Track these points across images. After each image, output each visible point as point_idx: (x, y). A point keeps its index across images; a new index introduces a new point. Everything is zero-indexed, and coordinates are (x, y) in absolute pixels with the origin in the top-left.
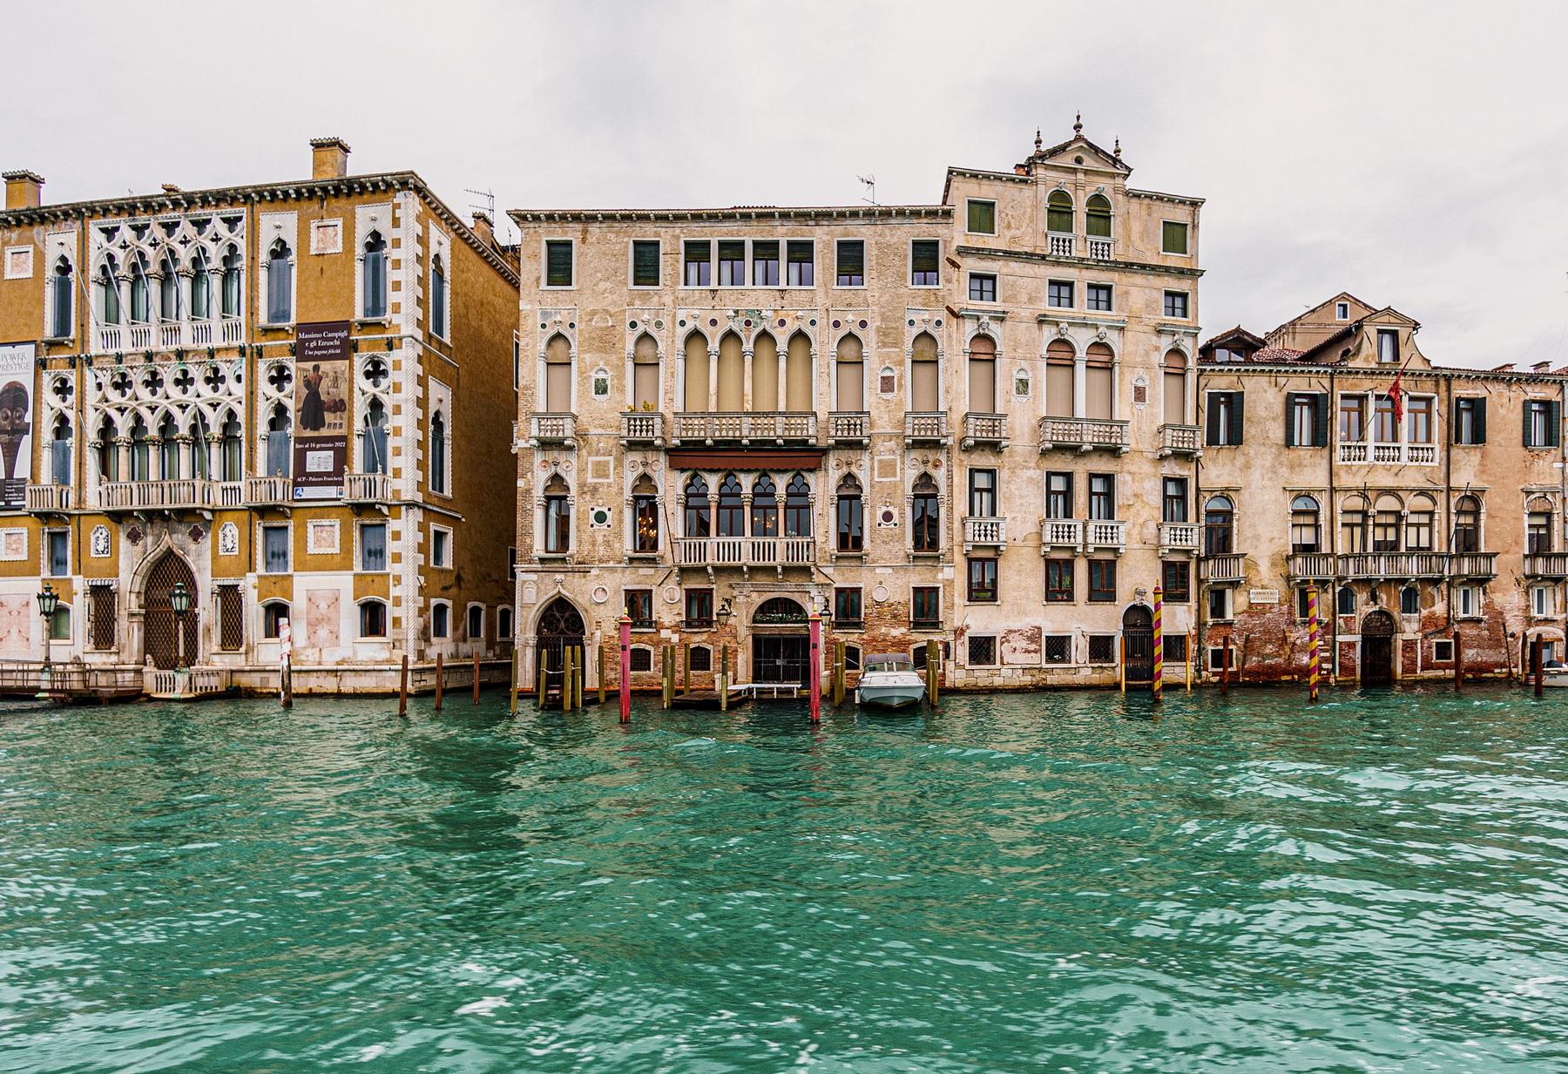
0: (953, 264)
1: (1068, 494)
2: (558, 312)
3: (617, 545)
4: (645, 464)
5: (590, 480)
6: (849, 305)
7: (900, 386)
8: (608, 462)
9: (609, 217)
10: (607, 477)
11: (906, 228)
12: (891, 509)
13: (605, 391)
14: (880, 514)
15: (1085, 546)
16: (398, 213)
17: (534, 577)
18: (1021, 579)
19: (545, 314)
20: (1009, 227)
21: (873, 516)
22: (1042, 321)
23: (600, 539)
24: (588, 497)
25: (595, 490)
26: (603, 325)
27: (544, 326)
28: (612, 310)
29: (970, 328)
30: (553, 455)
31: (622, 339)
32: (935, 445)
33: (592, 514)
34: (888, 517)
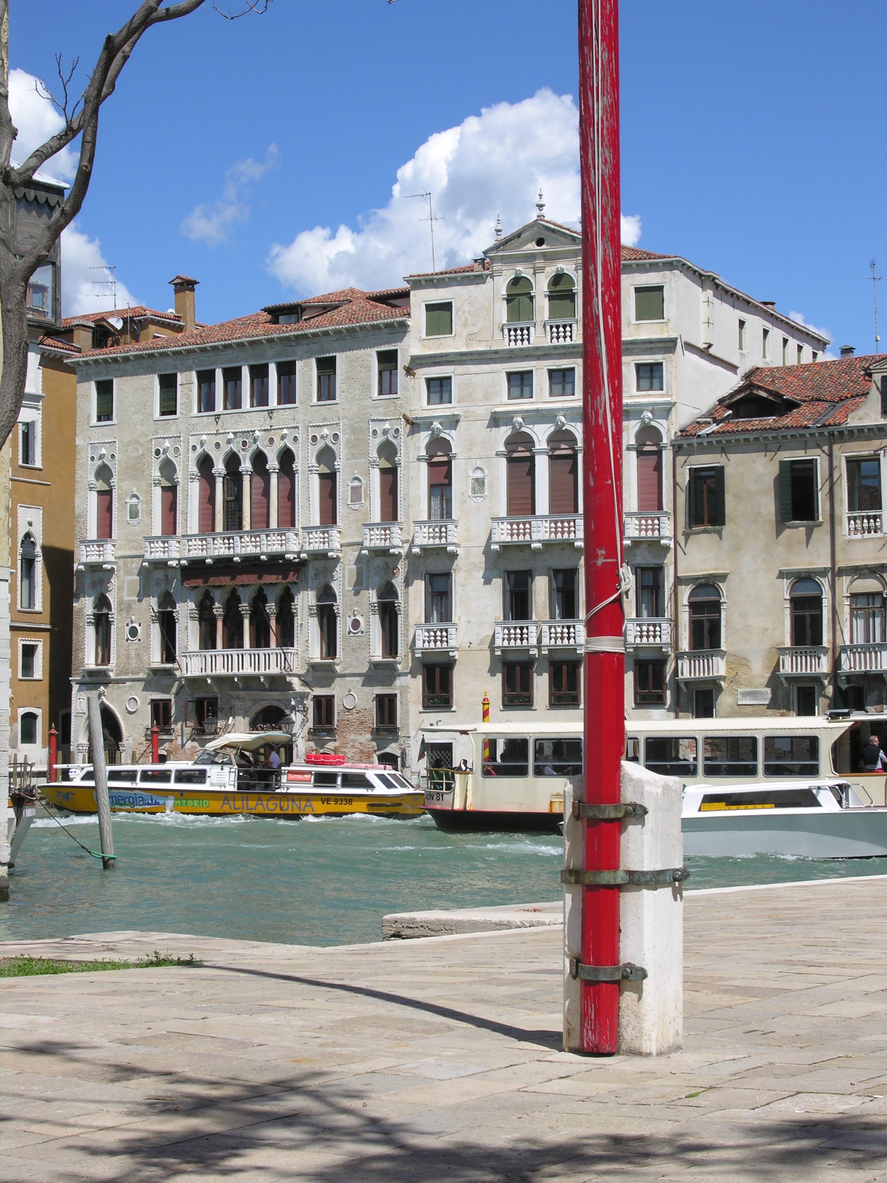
3: (145, 658)
5: (126, 598)
6: (324, 419)
12: (358, 617)
14: (349, 621)
18: (477, 683)
20: (465, 324)
21: (345, 623)
22: (496, 420)
23: (133, 653)
24: (124, 614)
26: (134, 454)
27: (93, 459)
28: (142, 440)
29: (424, 437)
34: (356, 624)
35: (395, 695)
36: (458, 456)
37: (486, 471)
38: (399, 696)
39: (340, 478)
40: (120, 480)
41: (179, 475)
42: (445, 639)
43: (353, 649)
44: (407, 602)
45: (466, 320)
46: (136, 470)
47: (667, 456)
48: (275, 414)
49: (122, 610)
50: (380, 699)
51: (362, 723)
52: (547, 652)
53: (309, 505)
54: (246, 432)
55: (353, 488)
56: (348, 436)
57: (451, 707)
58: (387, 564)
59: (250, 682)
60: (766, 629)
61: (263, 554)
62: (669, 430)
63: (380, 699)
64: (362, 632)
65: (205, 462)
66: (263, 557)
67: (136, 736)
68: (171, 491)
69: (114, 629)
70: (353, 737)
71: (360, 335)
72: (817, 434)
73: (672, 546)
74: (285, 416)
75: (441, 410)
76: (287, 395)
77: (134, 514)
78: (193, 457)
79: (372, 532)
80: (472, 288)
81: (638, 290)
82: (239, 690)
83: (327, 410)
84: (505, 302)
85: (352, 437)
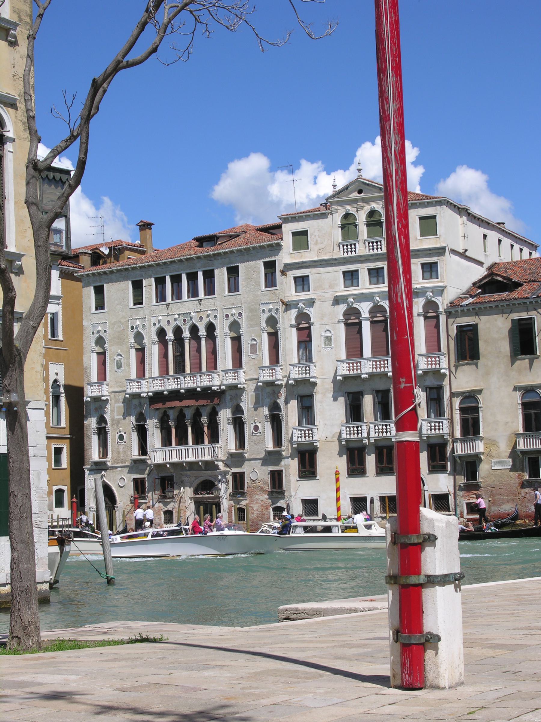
3: (129, 453)
5: (116, 417)
6: (233, 304)
14: (252, 426)
18: (331, 462)
20: (316, 243)
21: (249, 428)
22: (337, 301)
23: (121, 450)
24: (115, 427)
26: (119, 329)
27: (93, 333)
28: (123, 321)
29: (293, 313)
34: (256, 428)
35: (282, 470)
36: (315, 324)
37: (332, 332)
38: (284, 471)
40: (110, 346)
41: (146, 341)
42: (311, 435)
44: (287, 413)
45: (317, 241)
47: (443, 319)
48: (203, 302)
49: (114, 424)
50: (272, 473)
51: (262, 488)
52: (373, 441)
53: (225, 357)
54: (185, 313)
55: (251, 345)
56: (247, 314)
57: (316, 477)
58: (274, 391)
59: (193, 465)
60: (507, 423)
61: (198, 387)
62: (443, 303)
63: (272, 473)
64: (260, 433)
65: (161, 333)
66: (198, 389)
67: (125, 501)
68: (141, 351)
69: (109, 436)
70: (257, 497)
71: (252, 252)
72: (534, 302)
73: (448, 374)
74: (209, 303)
75: (304, 296)
76: (210, 290)
77: (119, 366)
78: (154, 330)
79: (264, 372)
80: (319, 221)
81: (421, 218)
82: (187, 471)
83: (234, 299)
84: (340, 229)
85: (250, 314)
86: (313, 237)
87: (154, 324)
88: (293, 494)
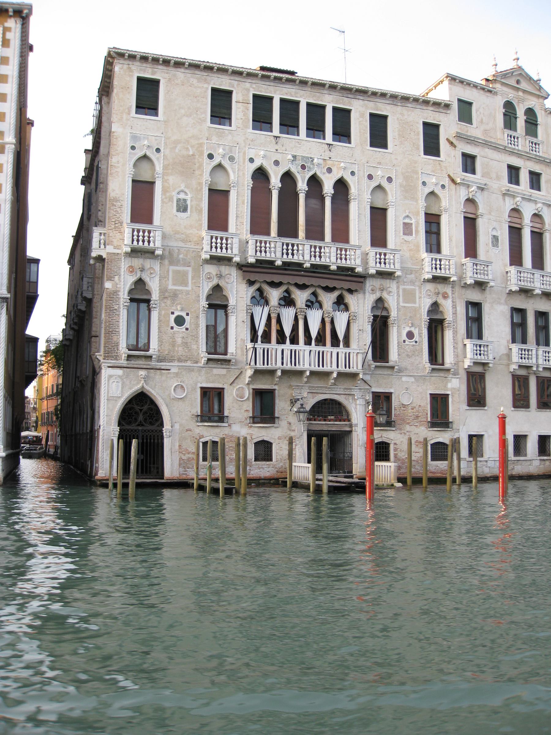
0: (452, 144)
1: (523, 325)
2: (146, 137)
3: (195, 347)
4: (220, 276)
5: (171, 287)
7: (417, 232)
8: (185, 274)
9: (195, 66)
10: (186, 285)
11: (418, 111)
12: (412, 329)
13: (185, 210)
15: (538, 366)
16: (9, 35)
17: (119, 372)
19: (135, 138)
23: (179, 341)
24: (169, 302)
25: (175, 295)
26: (185, 153)
27: (133, 148)
29: (463, 194)
30: (137, 262)
31: (201, 167)
32: (444, 280)
33: (173, 317)
34: (410, 335)
39: (391, 215)
42: (486, 353)
43: (408, 355)
45: (482, 120)
46: (186, 167)
51: (417, 417)
55: (405, 224)
64: (416, 342)
65: (261, 175)
85: (404, 183)
86: (478, 113)
87: (252, 160)
88: (461, 428)
